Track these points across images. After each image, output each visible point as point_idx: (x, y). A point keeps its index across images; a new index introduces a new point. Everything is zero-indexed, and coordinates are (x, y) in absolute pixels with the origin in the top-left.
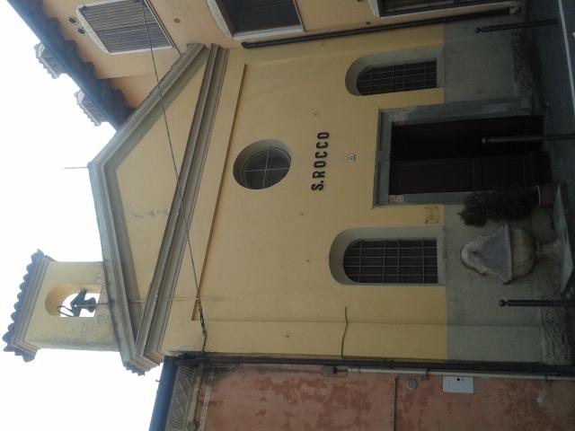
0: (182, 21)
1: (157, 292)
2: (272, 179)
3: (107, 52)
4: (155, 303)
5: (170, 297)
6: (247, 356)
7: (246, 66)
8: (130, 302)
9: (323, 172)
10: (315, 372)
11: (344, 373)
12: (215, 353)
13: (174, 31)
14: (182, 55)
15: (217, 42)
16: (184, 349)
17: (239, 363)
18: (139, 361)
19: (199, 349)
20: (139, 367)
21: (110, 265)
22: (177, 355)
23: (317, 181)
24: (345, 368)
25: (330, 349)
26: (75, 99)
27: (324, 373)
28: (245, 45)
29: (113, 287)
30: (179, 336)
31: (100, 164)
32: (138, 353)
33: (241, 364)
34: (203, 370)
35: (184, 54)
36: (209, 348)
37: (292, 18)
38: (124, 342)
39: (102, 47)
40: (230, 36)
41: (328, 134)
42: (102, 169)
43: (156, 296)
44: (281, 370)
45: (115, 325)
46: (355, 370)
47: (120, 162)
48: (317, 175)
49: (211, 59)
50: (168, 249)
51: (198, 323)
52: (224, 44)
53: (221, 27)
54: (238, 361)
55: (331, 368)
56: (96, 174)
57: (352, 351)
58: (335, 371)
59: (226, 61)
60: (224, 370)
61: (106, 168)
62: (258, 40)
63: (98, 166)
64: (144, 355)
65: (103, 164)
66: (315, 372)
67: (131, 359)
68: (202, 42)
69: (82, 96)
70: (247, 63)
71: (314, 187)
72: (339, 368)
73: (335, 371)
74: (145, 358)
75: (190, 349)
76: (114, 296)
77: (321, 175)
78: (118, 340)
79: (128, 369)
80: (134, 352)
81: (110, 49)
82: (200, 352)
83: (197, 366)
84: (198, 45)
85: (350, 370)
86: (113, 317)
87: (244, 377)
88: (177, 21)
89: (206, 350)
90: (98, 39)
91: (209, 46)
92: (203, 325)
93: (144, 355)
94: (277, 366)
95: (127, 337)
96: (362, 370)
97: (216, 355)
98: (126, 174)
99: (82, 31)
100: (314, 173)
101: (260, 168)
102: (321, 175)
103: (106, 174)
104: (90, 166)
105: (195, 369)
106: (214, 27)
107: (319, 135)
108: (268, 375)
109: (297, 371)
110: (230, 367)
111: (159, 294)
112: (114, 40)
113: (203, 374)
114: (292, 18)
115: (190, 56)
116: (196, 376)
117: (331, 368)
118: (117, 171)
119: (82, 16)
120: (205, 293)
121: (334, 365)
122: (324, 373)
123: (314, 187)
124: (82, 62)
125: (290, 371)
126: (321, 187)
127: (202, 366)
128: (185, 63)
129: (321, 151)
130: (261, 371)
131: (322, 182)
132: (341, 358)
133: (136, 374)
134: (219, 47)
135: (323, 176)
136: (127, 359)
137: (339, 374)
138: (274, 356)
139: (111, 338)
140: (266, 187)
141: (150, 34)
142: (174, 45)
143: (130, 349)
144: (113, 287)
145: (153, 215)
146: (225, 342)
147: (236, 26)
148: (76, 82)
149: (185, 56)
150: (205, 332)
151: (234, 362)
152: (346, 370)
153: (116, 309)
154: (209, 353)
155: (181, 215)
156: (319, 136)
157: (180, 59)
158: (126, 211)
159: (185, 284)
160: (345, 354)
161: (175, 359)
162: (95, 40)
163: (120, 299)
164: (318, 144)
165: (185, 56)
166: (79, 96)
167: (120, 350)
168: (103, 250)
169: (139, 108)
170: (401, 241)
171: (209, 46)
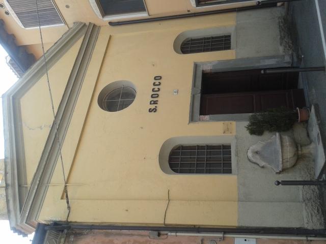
0: (71, 7)
1: (39, 179)
2: (124, 106)
3: (23, 27)
4: (36, 187)
5: (47, 183)
6: (98, 224)
7: (110, 37)
8: (20, 186)
9: (157, 101)
10: (145, 236)
11: (166, 236)
12: (76, 222)
13: (66, 14)
14: (70, 29)
15: (93, 22)
16: (54, 219)
17: (91, 229)
18: (23, 227)
19: (64, 219)
20: (23, 231)
21: (9, 161)
22: (49, 223)
23: (153, 107)
24: (166, 232)
25: (156, 219)
26: (5, 60)
27: (151, 237)
28: (111, 23)
29: (9, 176)
30: (51, 210)
31: (11, 94)
32: (22, 221)
33: (93, 230)
34: (66, 234)
35: (71, 28)
36: (72, 219)
37: (141, 8)
38: (12, 214)
39: (20, 24)
40: (100, 17)
41: (161, 77)
42: (11, 98)
43: (38, 182)
44: (120, 235)
45: (8, 201)
46: (173, 234)
47: (23, 94)
48: (152, 102)
49: (89, 32)
50: (49, 151)
51: (65, 201)
52: (97, 23)
53: (95, 11)
54: (92, 228)
55: (156, 233)
56: (6, 103)
57: (171, 221)
58: (159, 235)
59: (98, 33)
60: (81, 234)
61: (14, 98)
62: (119, 21)
63: (9, 96)
64: (26, 223)
65: (12, 96)
66: (145, 236)
67: (17, 225)
68: (83, 21)
69: (9, 58)
70: (111, 35)
71: (150, 111)
72: (162, 232)
73: (159, 235)
74: (26, 224)
75: (58, 219)
76: (9, 182)
77: (155, 103)
78: (9, 211)
79: (11, 230)
80: (19, 221)
81: (25, 25)
82: (65, 222)
83: (62, 231)
84: (82, 23)
85: (169, 234)
86: (7, 196)
87: (94, 239)
88: (67, 7)
89: (69, 220)
90: (20, 21)
91: (87, 24)
92: (68, 202)
93: (26, 223)
94: (118, 231)
95: (15, 210)
96: (178, 234)
97: (76, 224)
98: (27, 103)
99: (7, 13)
100: (151, 102)
101: (115, 99)
102: (155, 103)
103: (14, 101)
104: (3, 96)
105: (60, 233)
106: (92, 12)
107: (155, 77)
108: (111, 238)
109: (132, 235)
110: (85, 232)
111: (39, 181)
112: (30, 19)
113: (67, 237)
114: (141, 8)
115: (74, 30)
116: (61, 238)
117: (156, 233)
118: (21, 100)
119: (7, 3)
120: (72, 180)
121: (159, 230)
122: (151, 237)
123: (150, 111)
124: (7, 34)
125: (129, 235)
126: (155, 110)
127: (66, 231)
128: (72, 33)
129: (156, 88)
130: (107, 235)
131: (156, 107)
132: (164, 226)
133: (21, 236)
134: (94, 26)
135: (157, 103)
136: (14, 225)
137: (162, 237)
138: (116, 225)
139: (6, 211)
140: (119, 110)
141: (51, 16)
142: (66, 23)
143: (16, 219)
144: (9, 176)
145: (41, 129)
146: (81, 216)
147: (105, 11)
148: (4, 47)
149: (72, 30)
150: (69, 208)
151: (88, 229)
152: (167, 234)
153: (10, 191)
154: (71, 222)
155: (60, 126)
156: (155, 78)
157: (68, 31)
158: (24, 125)
159: (57, 176)
160: (166, 223)
161: (45, 225)
162: (15, 19)
163: (13, 185)
164: (154, 83)
165: (72, 30)
166: (8, 58)
167: (9, 218)
168: (5, 151)
169: (38, 60)
170: (198, 146)
171: (87, 24)
